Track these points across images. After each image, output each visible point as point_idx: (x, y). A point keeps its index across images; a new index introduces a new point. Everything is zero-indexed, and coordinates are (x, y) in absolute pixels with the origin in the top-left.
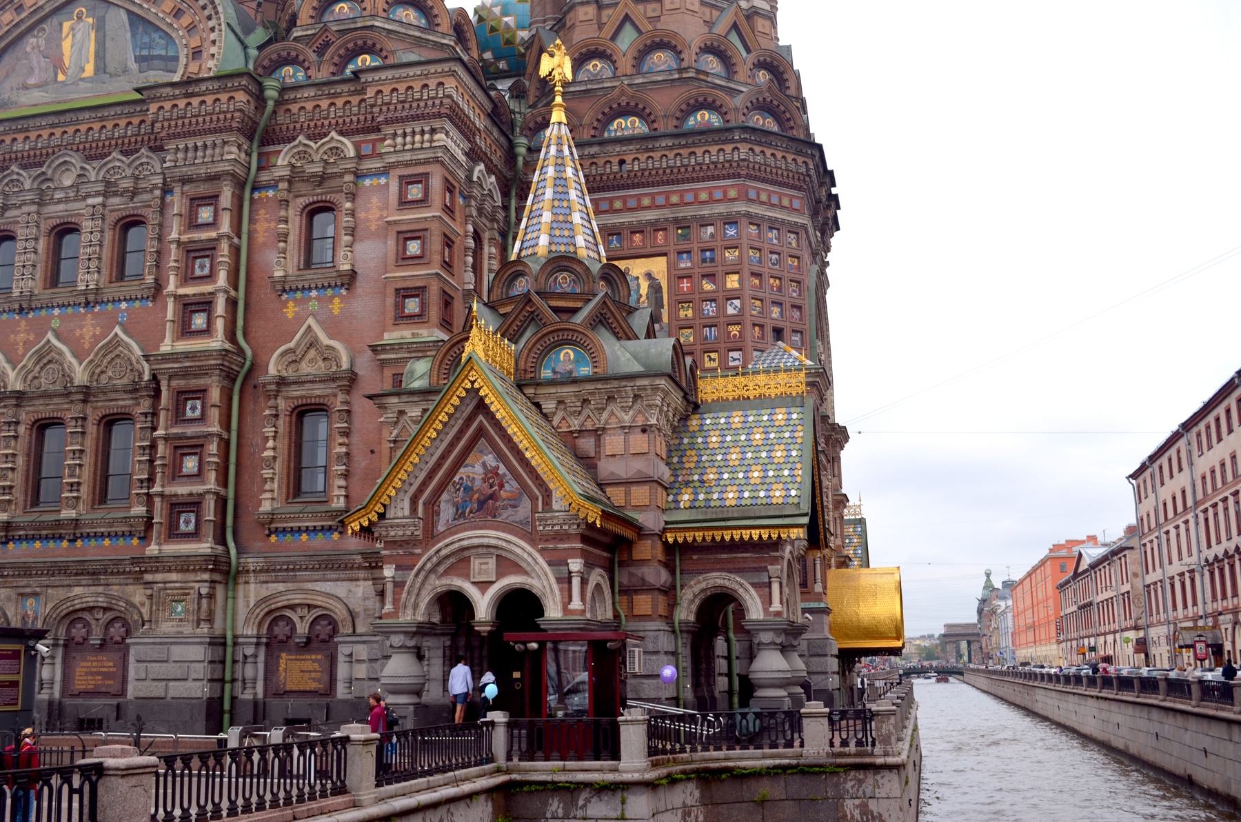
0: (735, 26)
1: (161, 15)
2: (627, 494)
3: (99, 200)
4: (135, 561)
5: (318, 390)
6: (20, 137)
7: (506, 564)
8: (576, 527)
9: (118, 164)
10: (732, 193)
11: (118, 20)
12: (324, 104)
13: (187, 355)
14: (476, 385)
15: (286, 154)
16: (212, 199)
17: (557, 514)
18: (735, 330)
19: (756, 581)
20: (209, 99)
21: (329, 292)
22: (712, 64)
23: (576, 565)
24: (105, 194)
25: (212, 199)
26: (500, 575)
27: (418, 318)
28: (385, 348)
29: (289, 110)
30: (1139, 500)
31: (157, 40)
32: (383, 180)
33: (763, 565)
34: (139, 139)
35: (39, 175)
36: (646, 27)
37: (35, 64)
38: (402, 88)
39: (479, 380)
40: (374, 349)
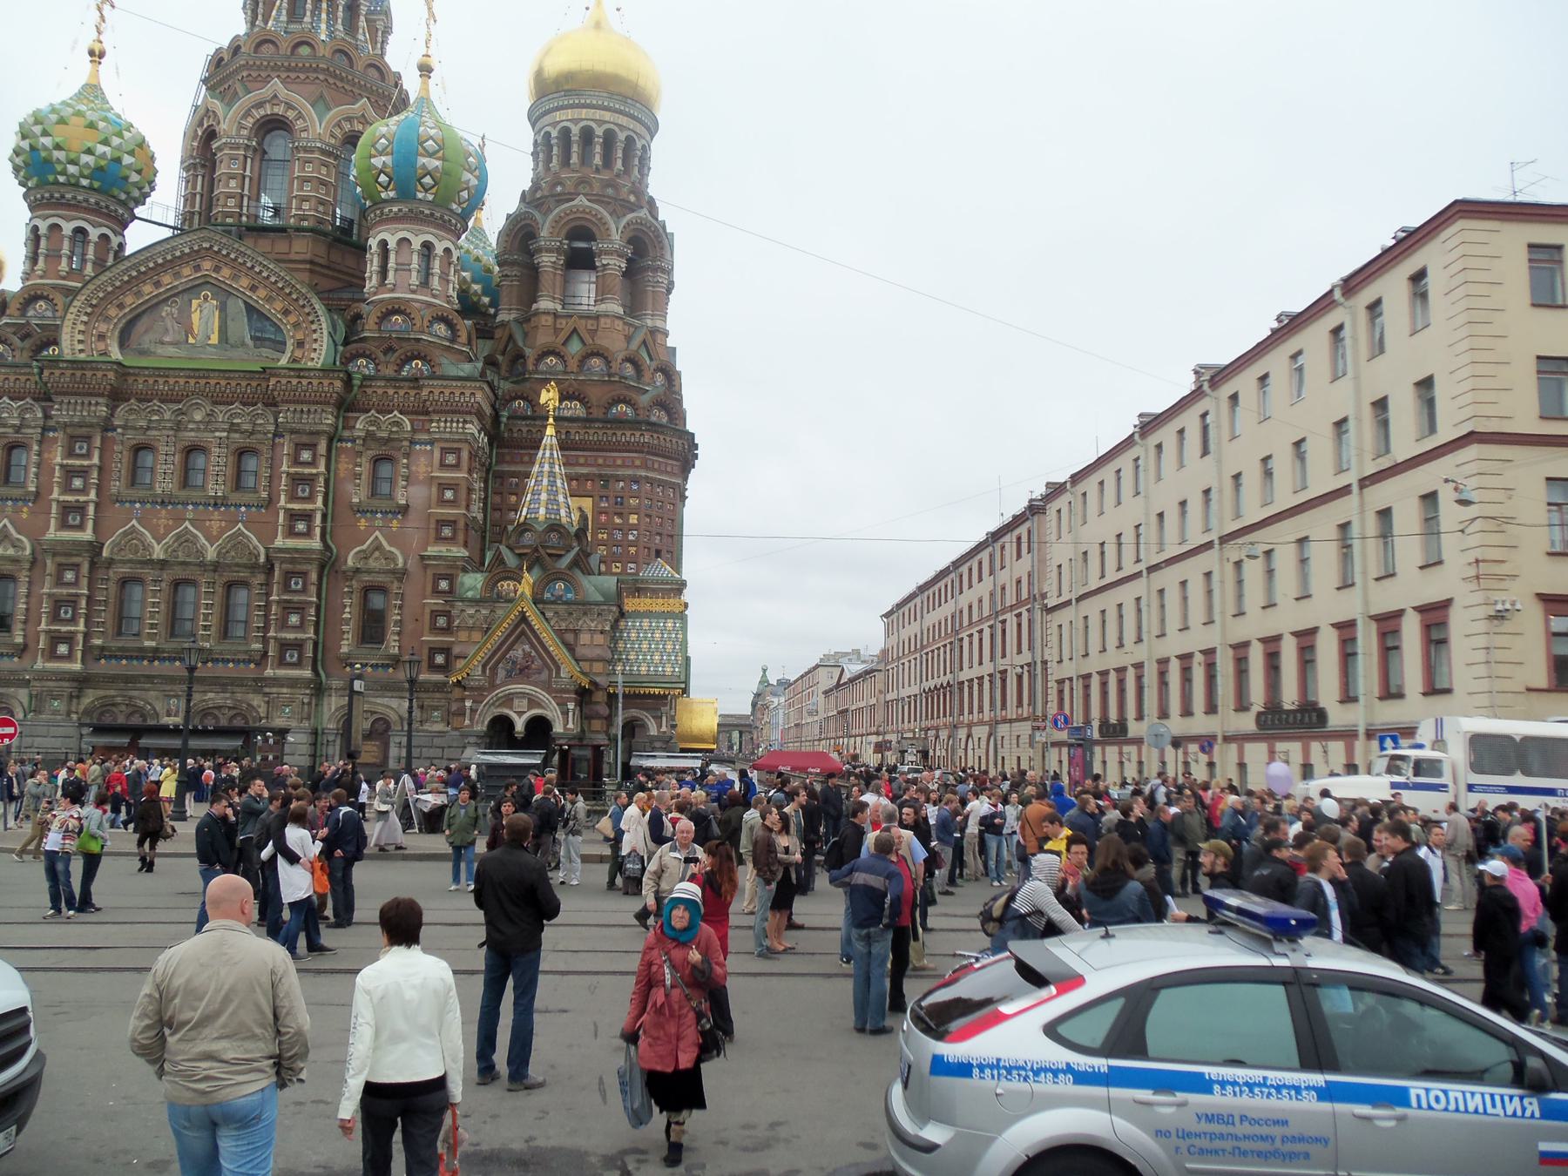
0: (644, 342)
2: (591, 666)
3: (225, 434)
4: (255, 680)
5: (381, 578)
6: (161, 381)
7: (533, 703)
10: (638, 463)
11: (236, 307)
12: (391, 392)
13: (296, 550)
16: (312, 447)
18: (632, 550)
20: (315, 382)
21: (390, 516)
22: (629, 370)
23: (571, 706)
24: (229, 431)
25: (312, 447)
26: (530, 708)
27: (451, 540)
28: (429, 557)
30: (887, 635)
32: (428, 448)
36: (589, 340)
38: (447, 392)
40: (423, 558)
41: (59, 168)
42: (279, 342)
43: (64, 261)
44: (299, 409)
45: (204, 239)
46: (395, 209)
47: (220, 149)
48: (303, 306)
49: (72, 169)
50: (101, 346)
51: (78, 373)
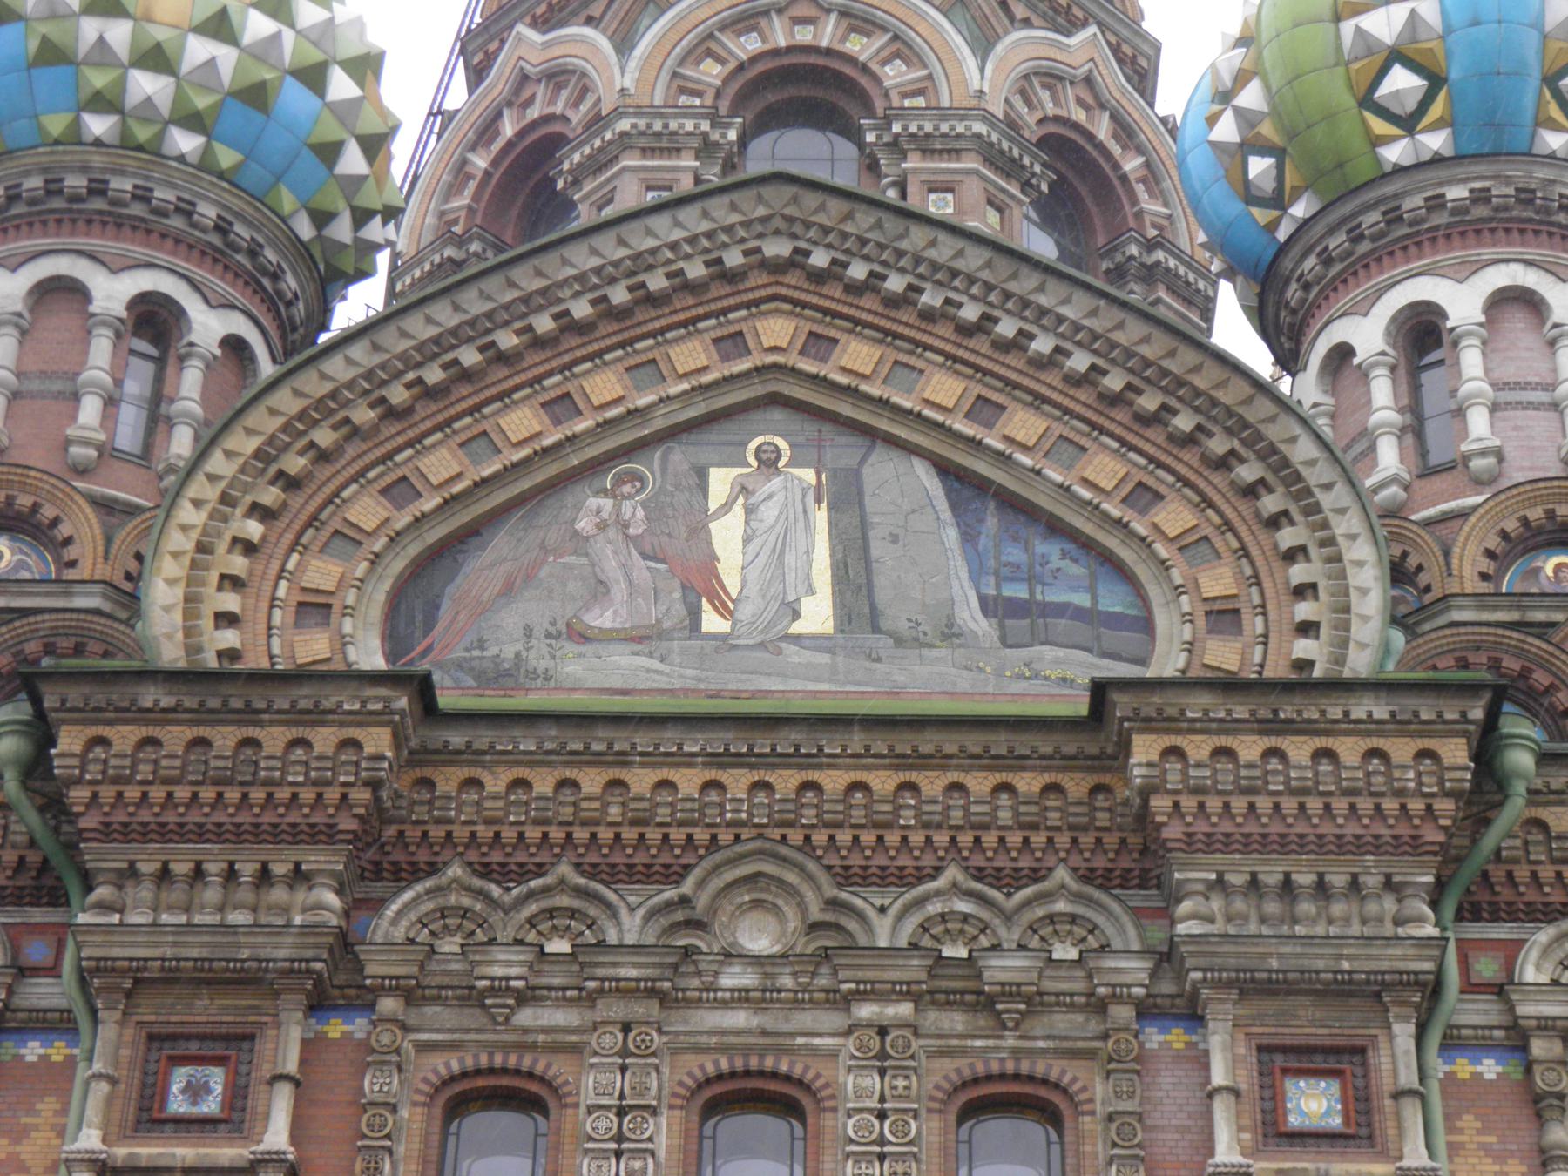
1: (1086, 494)
3: (905, 1009)
9: (963, 906)
15: (1546, 951)
29: (1542, 825)
31: (1055, 561)
34: (1038, 839)
35: (669, 906)
37: (611, 567)
41: (99, 79)
42: (1114, 621)
43: (90, 410)
44: (1271, 876)
45: (765, 226)
46: (1456, 193)
47: (597, 164)
48: (1223, 463)
49: (146, 85)
50: (314, 647)
51: (225, 738)
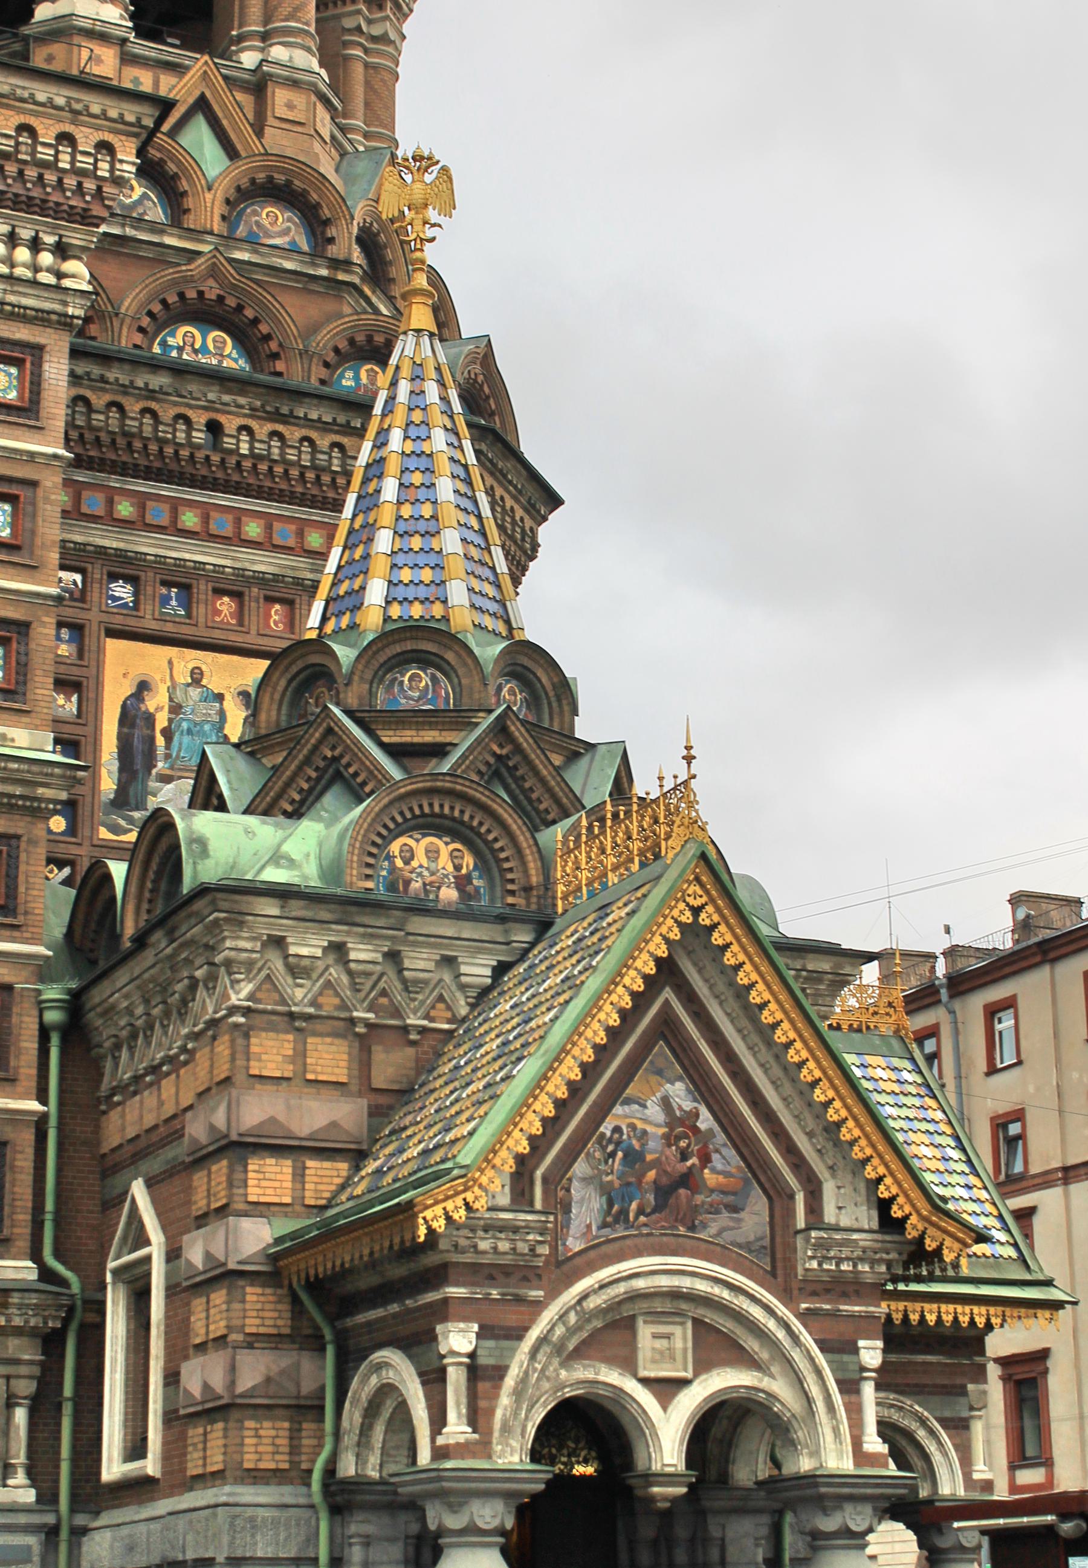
8: (883, 1268)
14: (704, 919)
17: (855, 1236)
19: (947, 1414)
26: (703, 1366)
33: (958, 1381)
39: (710, 909)
